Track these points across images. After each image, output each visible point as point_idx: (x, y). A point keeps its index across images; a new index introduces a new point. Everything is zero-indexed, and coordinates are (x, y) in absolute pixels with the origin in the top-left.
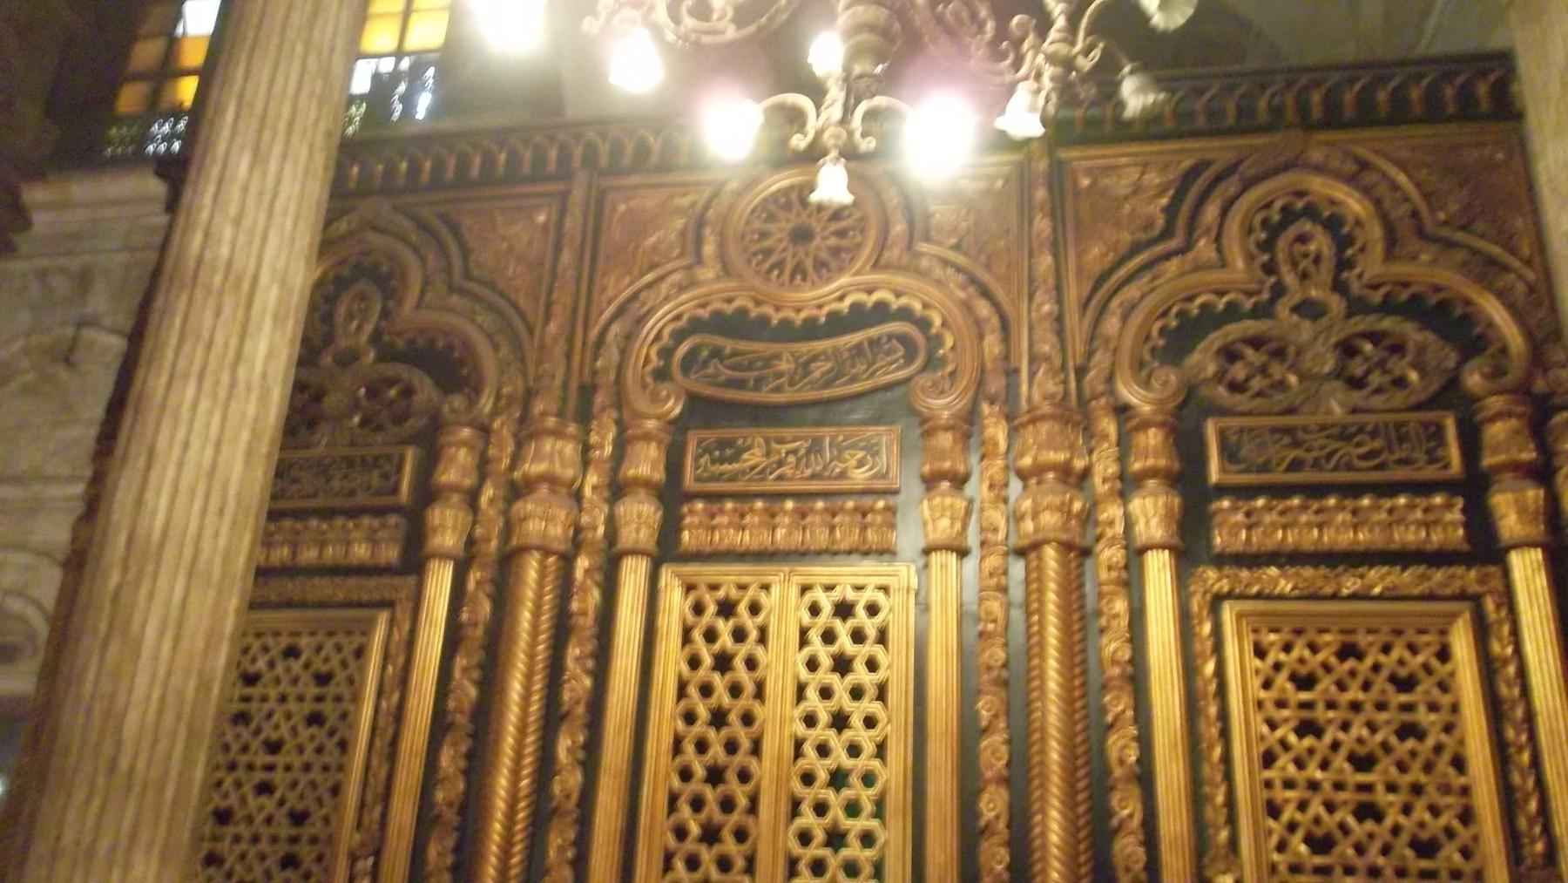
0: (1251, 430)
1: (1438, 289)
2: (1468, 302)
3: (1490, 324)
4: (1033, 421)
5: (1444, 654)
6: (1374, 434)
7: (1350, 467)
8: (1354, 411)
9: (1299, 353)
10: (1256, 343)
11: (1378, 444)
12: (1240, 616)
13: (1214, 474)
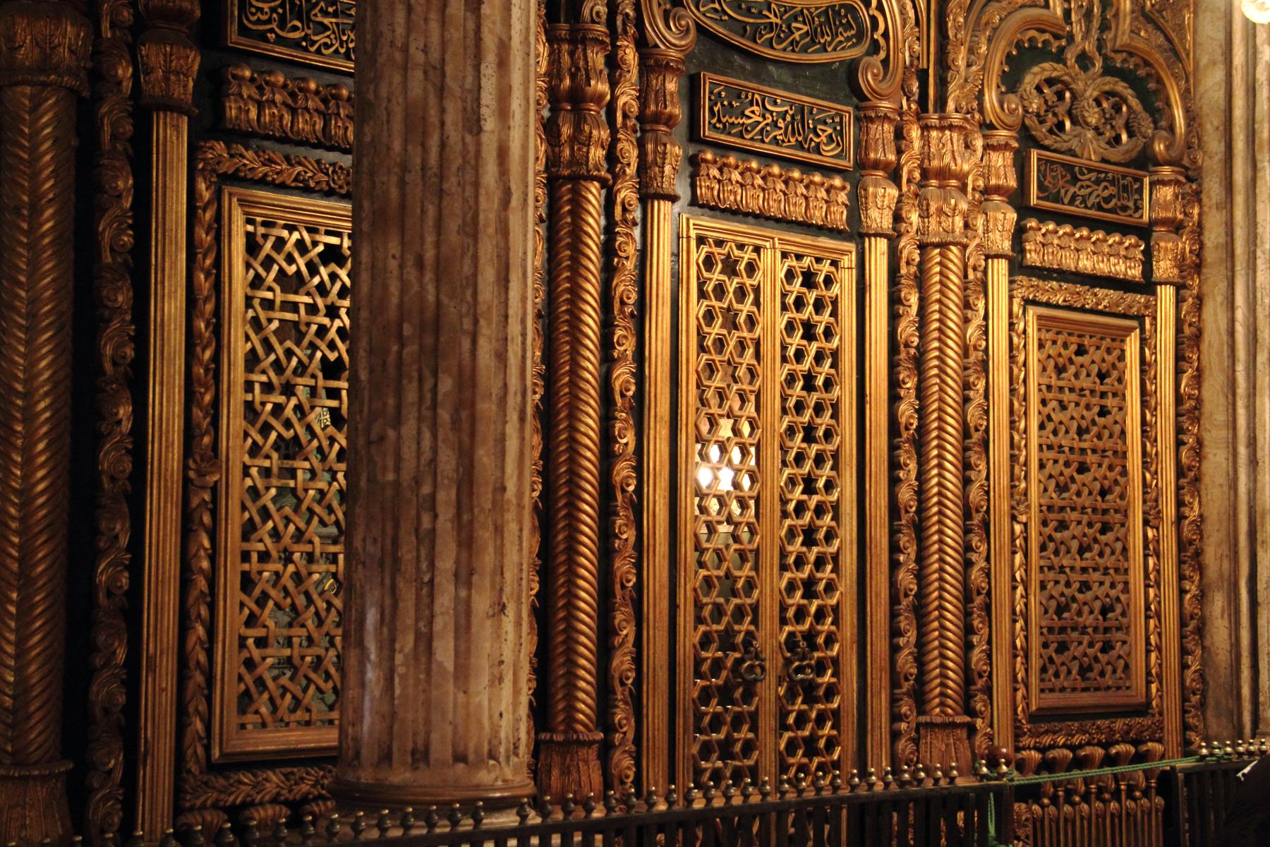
0: (1053, 163)
1: (1147, 63)
2: (1159, 81)
3: (1168, 104)
4: (942, 129)
5: (1122, 358)
6: (1112, 182)
7: (1100, 208)
8: (1104, 160)
9: (1074, 97)
10: (1050, 82)
11: (1112, 190)
12: (1040, 317)
13: (1034, 201)
